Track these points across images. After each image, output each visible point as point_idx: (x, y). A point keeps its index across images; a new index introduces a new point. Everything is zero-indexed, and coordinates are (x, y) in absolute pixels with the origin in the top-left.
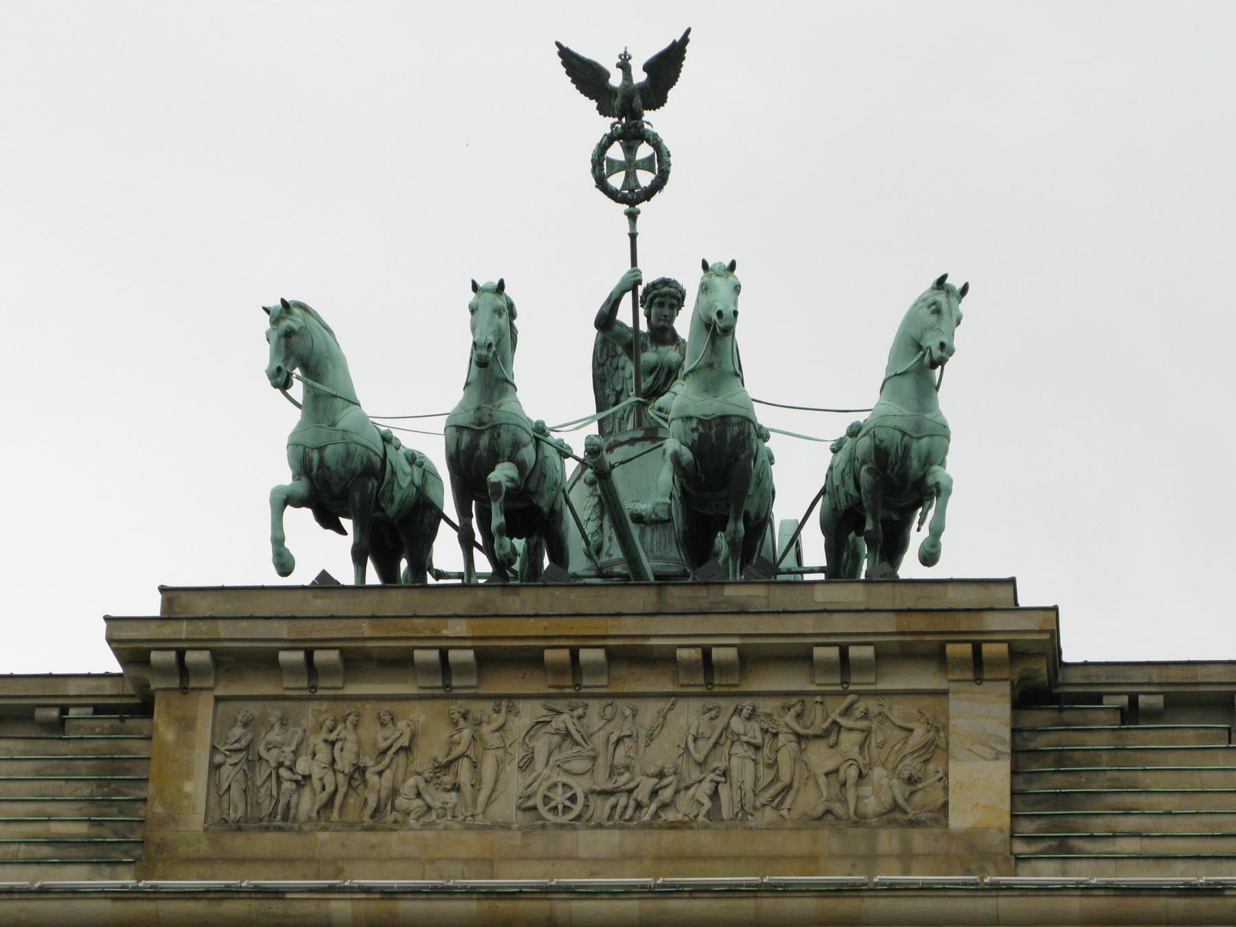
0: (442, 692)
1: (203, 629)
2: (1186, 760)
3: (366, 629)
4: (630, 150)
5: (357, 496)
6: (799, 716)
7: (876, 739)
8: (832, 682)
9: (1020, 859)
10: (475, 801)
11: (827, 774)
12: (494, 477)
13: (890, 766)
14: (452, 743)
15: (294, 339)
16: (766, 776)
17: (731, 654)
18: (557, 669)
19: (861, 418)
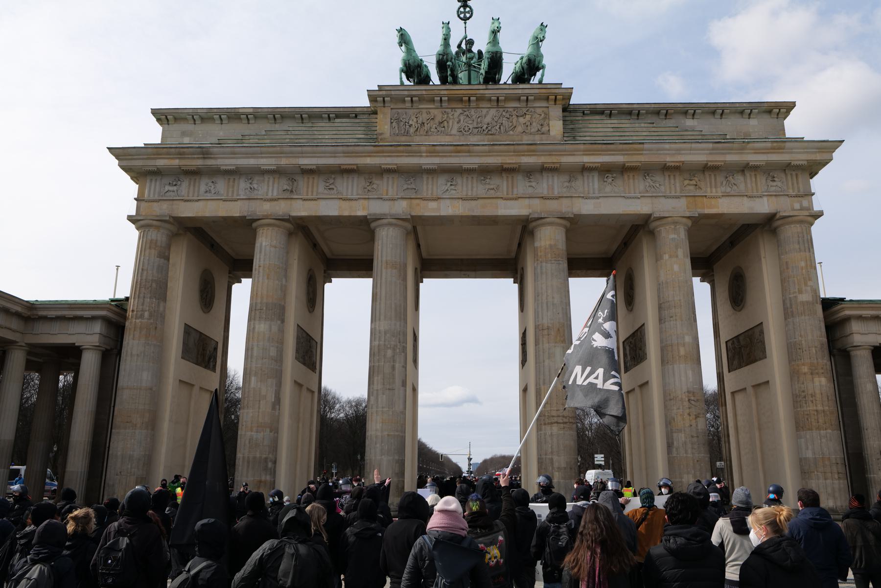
0: (440, 107)
1: (389, 93)
2: (597, 122)
3: (424, 92)
4: (465, 9)
5: (416, 71)
6: (517, 112)
7: (533, 117)
8: (524, 104)
9: (565, 141)
10: (448, 129)
11: (524, 124)
13: (537, 122)
14: (443, 118)
15: (403, 36)
16: (511, 124)
17: (503, 98)
18: (465, 102)
19: (523, 55)
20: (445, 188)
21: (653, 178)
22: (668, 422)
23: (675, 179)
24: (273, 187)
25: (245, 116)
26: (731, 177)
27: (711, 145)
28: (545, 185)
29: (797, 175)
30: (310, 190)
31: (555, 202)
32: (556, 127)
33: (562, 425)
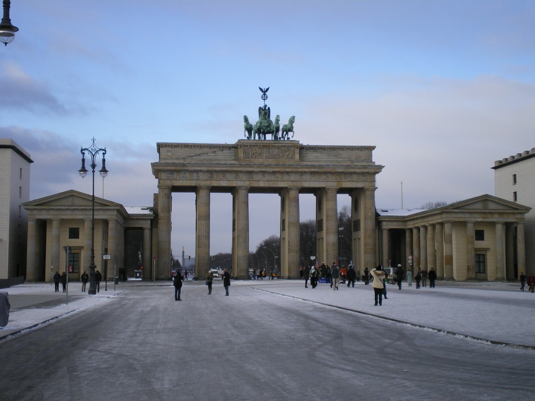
1: (243, 144)
4: (264, 96)
12: (262, 131)
16: (282, 155)
20: (261, 177)
21: (327, 175)
22: (327, 251)
23: (333, 175)
24: (205, 176)
25: (190, 146)
26: (351, 176)
27: (345, 167)
28: (293, 177)
29: (371, 175)
30: (217, 177)
31: (296, 182)
32: (297, 156)
33: (296, 253)
